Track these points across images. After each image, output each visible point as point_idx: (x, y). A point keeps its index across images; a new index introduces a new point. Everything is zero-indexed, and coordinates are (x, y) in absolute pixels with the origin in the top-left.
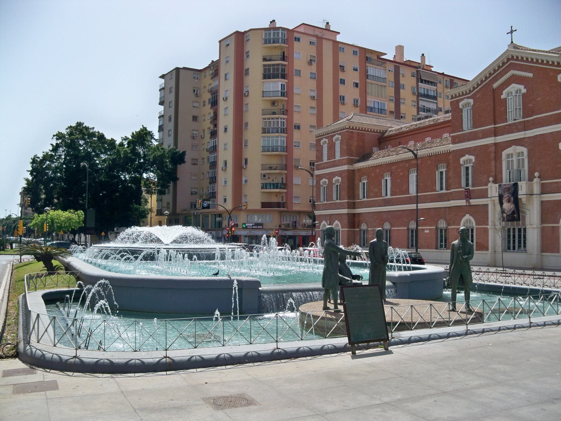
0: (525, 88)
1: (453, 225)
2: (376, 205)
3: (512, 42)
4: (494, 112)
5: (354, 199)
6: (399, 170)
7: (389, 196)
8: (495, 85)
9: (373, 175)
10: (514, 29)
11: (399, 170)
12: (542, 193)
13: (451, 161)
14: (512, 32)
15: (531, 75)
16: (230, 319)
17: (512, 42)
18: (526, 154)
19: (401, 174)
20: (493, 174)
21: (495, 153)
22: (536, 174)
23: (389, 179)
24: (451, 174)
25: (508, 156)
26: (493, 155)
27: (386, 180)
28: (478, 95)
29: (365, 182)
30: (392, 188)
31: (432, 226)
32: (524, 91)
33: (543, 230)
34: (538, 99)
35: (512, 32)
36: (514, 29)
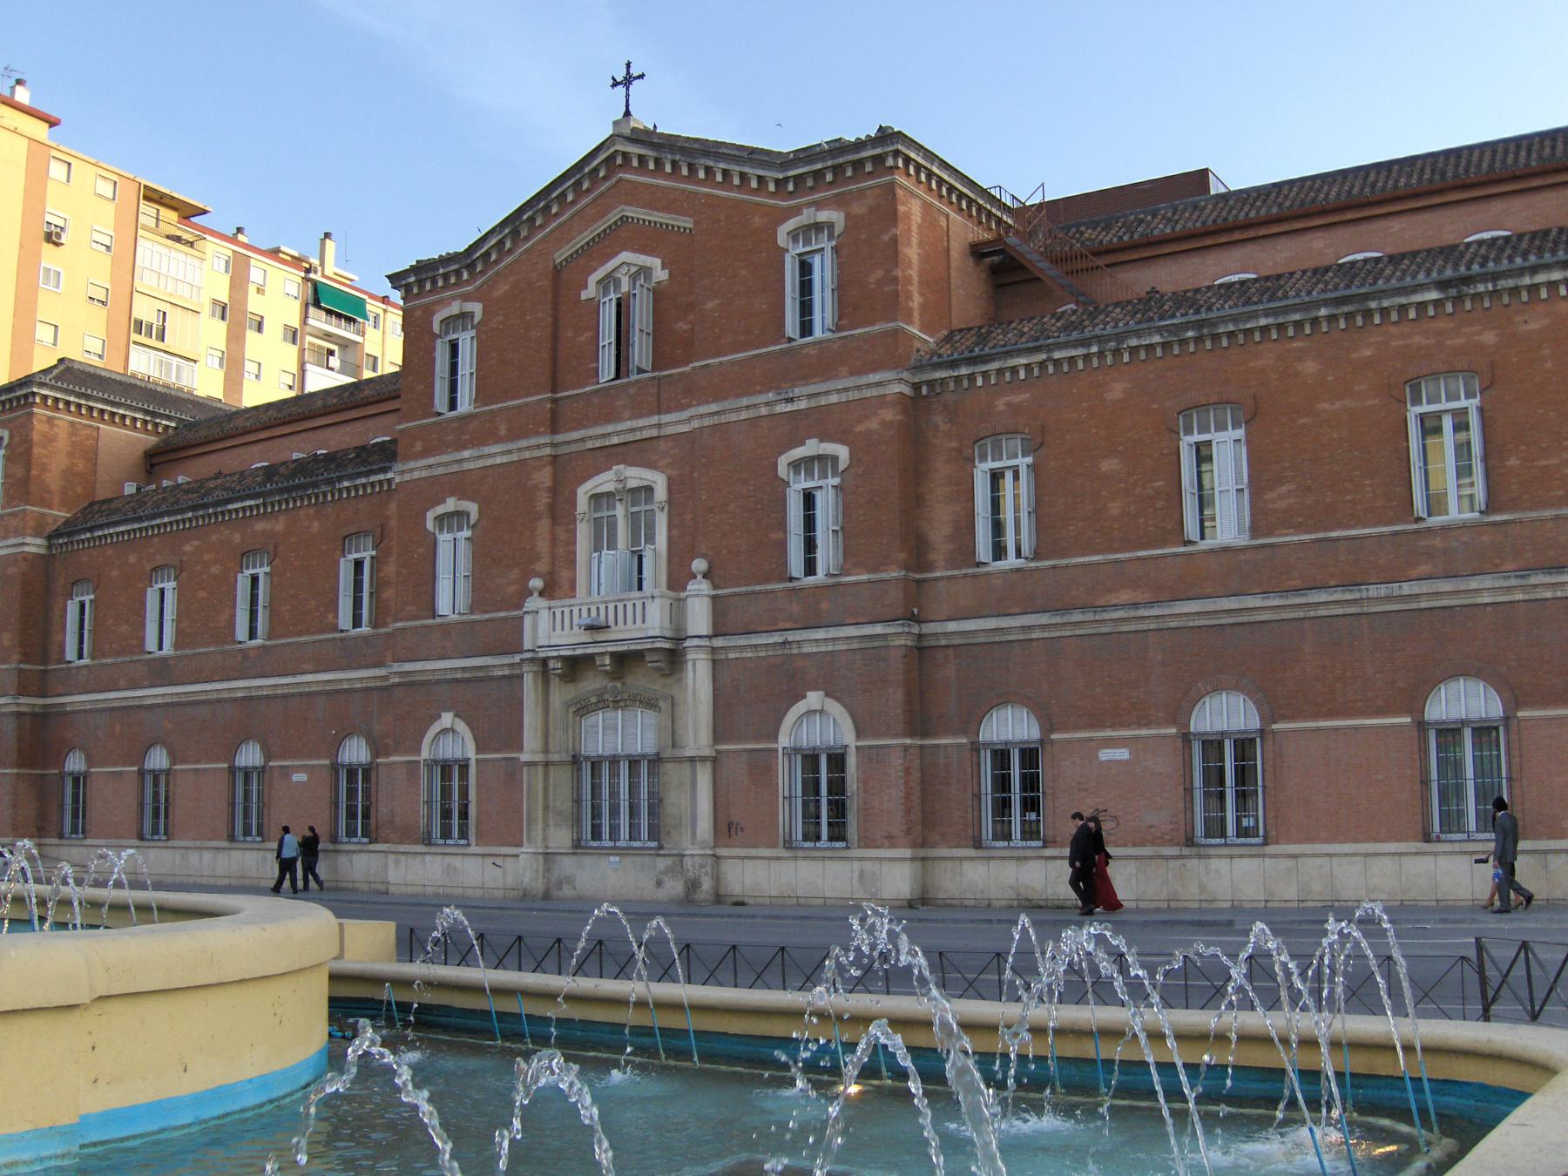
0: (663, 268)
1: (396, 752)
2: (122, 683)
3: (627, 113)
4: (554, 348)
5: (45, 661)
6: (206, 557)
7: (168, 650)
8: (560, 256)
9: (115, 573)
10: (635, 72)
11: (206, 557)
12: (715, 635)
13: (393, 523)
14: (628, 81)
15: (687, 223)
16: (26, 658)
17: (627, 113)
18: (661, 493)
19: (215, 570)
20: (543, 566)
21: (554, 491)
22: (699, 565)
23: (170, 586)
24: (390, 569)
25: (596, 498)
26: (543, 499)
27: (162, 591)
28: (502, 289)
29: (87, 598)
30: (179, 620)
31: (318, 758)
32: (661, 275)
33: (843, 771)
34: (710, 305)
35: (628, 81)
36: (635, 72)
